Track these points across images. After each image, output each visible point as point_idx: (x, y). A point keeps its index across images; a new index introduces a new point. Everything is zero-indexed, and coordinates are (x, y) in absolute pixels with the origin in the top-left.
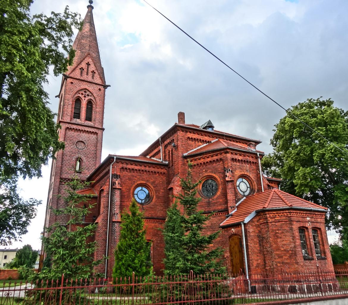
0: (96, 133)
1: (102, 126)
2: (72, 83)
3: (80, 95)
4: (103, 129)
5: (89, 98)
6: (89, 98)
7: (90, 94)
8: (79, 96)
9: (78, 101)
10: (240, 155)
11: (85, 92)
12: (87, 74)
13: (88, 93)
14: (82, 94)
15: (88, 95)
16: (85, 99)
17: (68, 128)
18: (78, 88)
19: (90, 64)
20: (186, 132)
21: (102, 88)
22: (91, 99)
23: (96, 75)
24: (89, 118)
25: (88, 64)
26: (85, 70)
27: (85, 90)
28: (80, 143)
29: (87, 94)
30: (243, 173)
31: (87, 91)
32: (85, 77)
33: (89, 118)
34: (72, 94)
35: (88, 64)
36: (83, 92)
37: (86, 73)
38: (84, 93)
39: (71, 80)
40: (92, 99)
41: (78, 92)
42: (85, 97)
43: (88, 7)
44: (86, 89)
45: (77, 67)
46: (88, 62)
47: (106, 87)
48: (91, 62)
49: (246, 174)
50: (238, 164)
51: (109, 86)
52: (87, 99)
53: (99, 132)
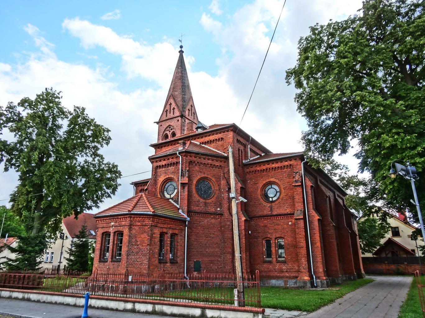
5: (173, 131)
6: (173, 131)
10: (164, 160)
12: (170, 113)
15: (172, 129)
18: (165, 127)
20: (162, 147)
26: (169, 110)
29: (171, 129)
30: (167, 176)
36: (169, 129)
37: (169, 113)
41: (165, 130)
44: (170, 125)
49: (170, 176)
50: (164, 169)
52: (171, 132)
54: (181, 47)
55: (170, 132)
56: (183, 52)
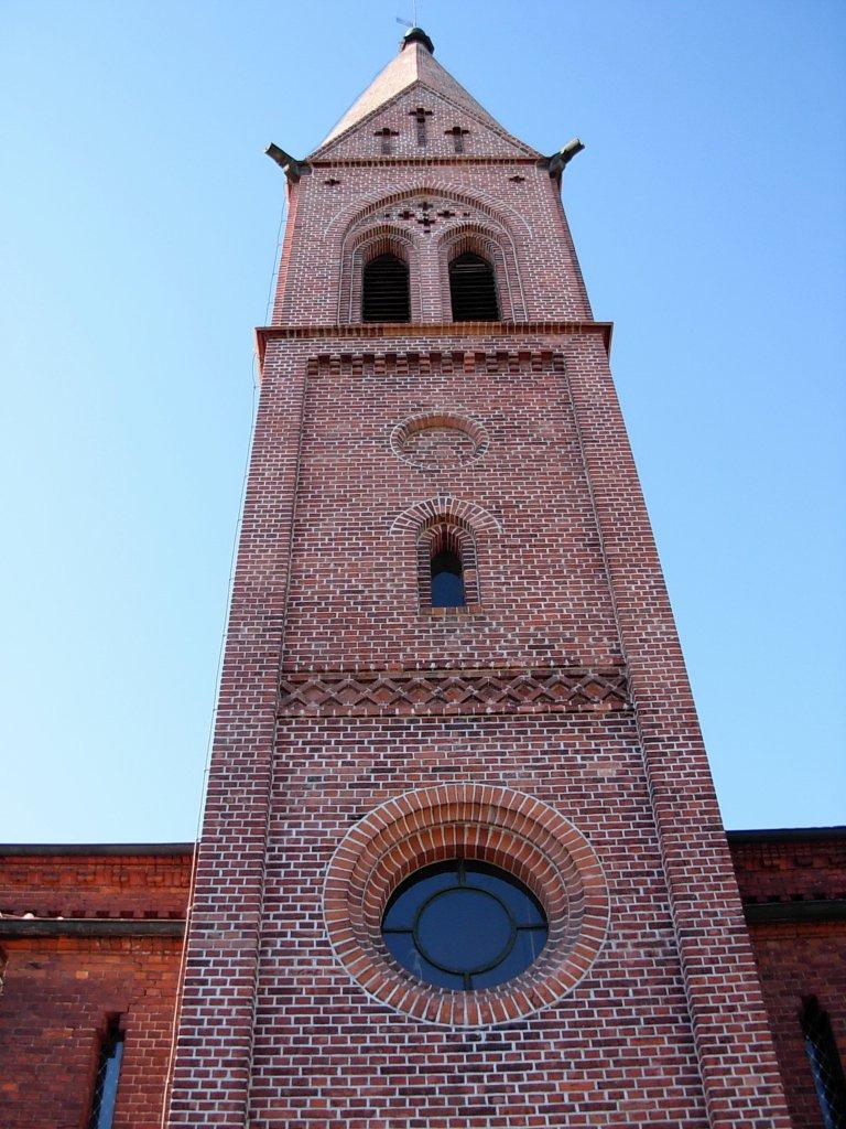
0: (547, 356)
1: (587, 309)
2: (332, 183)
3: (396, 222)
4: (606, 330)
8: (388, 229)
11: (425, 206)
14: (406, 215)
16: (427, 232)
17: (324, 360)
19: (430, 113)
21: (537, 175)
22: (467, 227)
28: (425, 442)
31: (429, 199)
32: (405, 144)
34: (341, 216)
39: (327, 174)
40: (477, 219)
42: (426, 222)
47: (554, 166)
52: (442, 226)
53: (581, 355)
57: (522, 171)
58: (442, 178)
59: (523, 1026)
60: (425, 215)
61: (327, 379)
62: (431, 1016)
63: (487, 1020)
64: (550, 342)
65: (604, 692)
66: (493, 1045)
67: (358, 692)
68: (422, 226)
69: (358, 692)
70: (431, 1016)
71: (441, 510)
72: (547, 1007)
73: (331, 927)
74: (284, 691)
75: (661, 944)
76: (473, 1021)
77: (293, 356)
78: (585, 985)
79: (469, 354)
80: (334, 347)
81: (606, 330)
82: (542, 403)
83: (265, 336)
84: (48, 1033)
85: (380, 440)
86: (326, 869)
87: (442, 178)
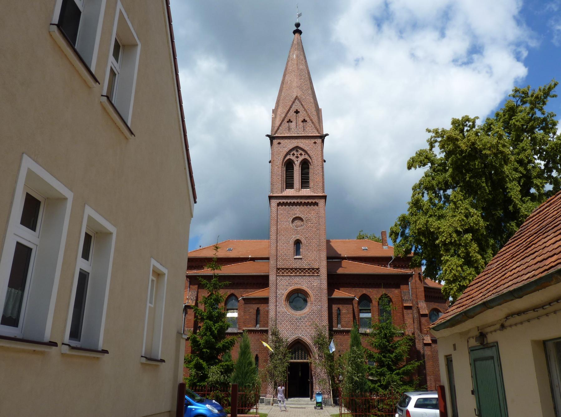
2: (279, 143)
7: (303, 153)
9: (289, 165)
11: (297, 151)
13: (300, 151)
15: (301, 154)
16: (297, 161)
17: (280, 203)
19: (299, 112)
23: (309, 123)
24: (305, 183)
25: (297, 112)
27: (297, 148)
33: (305, 183)
35: (297, 112)
38: (296, 153)
39: (279, 141)
40: (307, 157)
41: (288, 153)
42: (297, 157)
43: (295, 32)
45: (283, 120)
46: (297, 110)
47: (322, 137)
48: (300, 109)
51: (327, 135)
52: (301, 158)
54: (298, 25)
55: (297, 157)
56: (300, 32)
57: (316, 140)
58: (301, 143)
59: (303, 317)
60: (297, 154)
61: (280, 207)
62: (294, 316)
63: (300, 316)
64: (317, 201)
65: (316, 272)
66: (300, 319)
67: (286, 271)
68: (296, 158)
69: (286, 271)
70: (294, 316)
71: (297, 238)
72: (306, 315)
73: (284, 305)
74: (277, 271)
75: (319, 308)
76: (298, 316)
77: (274, 202)
78: (310, 312)
79: (303, 202)
80: (281, 201)
81: (325, 197)
82: (314, 213)
83: (270, 198)
84: (251, 310)
85: (289, 222)
86: (283, 297)
87: (301, 143)
